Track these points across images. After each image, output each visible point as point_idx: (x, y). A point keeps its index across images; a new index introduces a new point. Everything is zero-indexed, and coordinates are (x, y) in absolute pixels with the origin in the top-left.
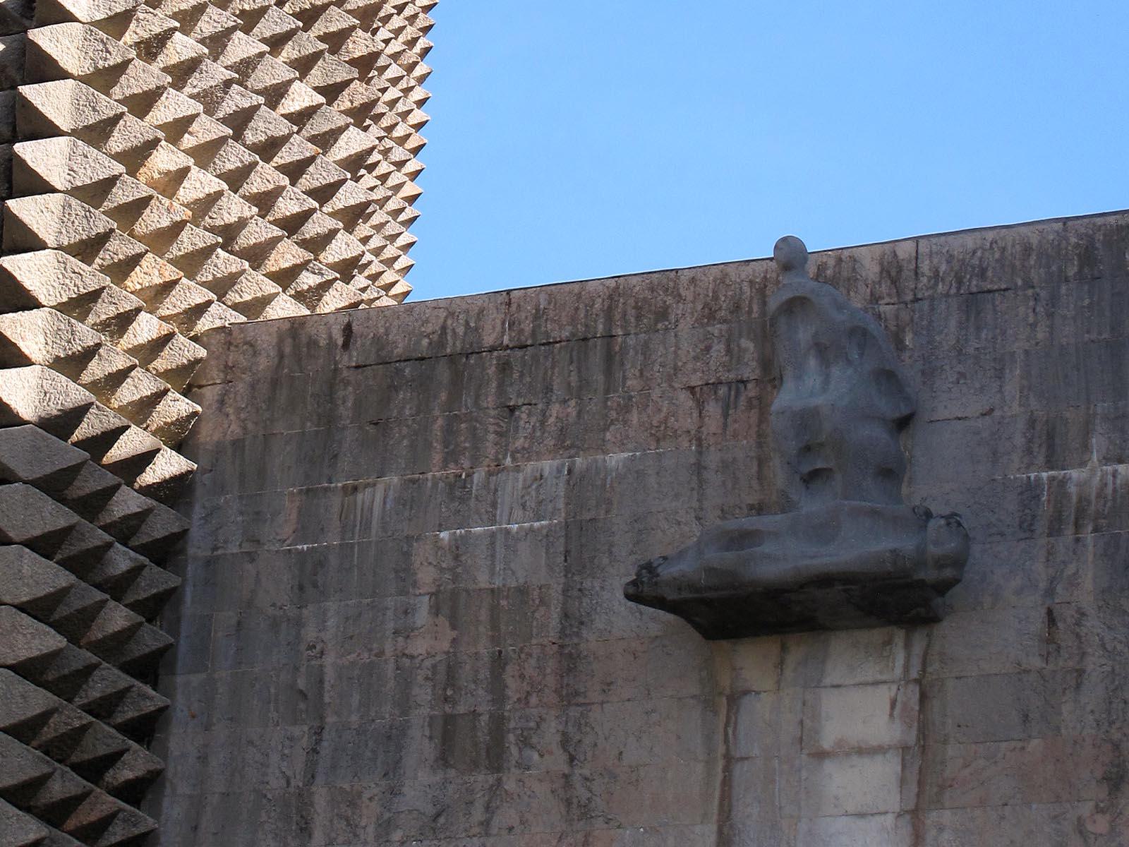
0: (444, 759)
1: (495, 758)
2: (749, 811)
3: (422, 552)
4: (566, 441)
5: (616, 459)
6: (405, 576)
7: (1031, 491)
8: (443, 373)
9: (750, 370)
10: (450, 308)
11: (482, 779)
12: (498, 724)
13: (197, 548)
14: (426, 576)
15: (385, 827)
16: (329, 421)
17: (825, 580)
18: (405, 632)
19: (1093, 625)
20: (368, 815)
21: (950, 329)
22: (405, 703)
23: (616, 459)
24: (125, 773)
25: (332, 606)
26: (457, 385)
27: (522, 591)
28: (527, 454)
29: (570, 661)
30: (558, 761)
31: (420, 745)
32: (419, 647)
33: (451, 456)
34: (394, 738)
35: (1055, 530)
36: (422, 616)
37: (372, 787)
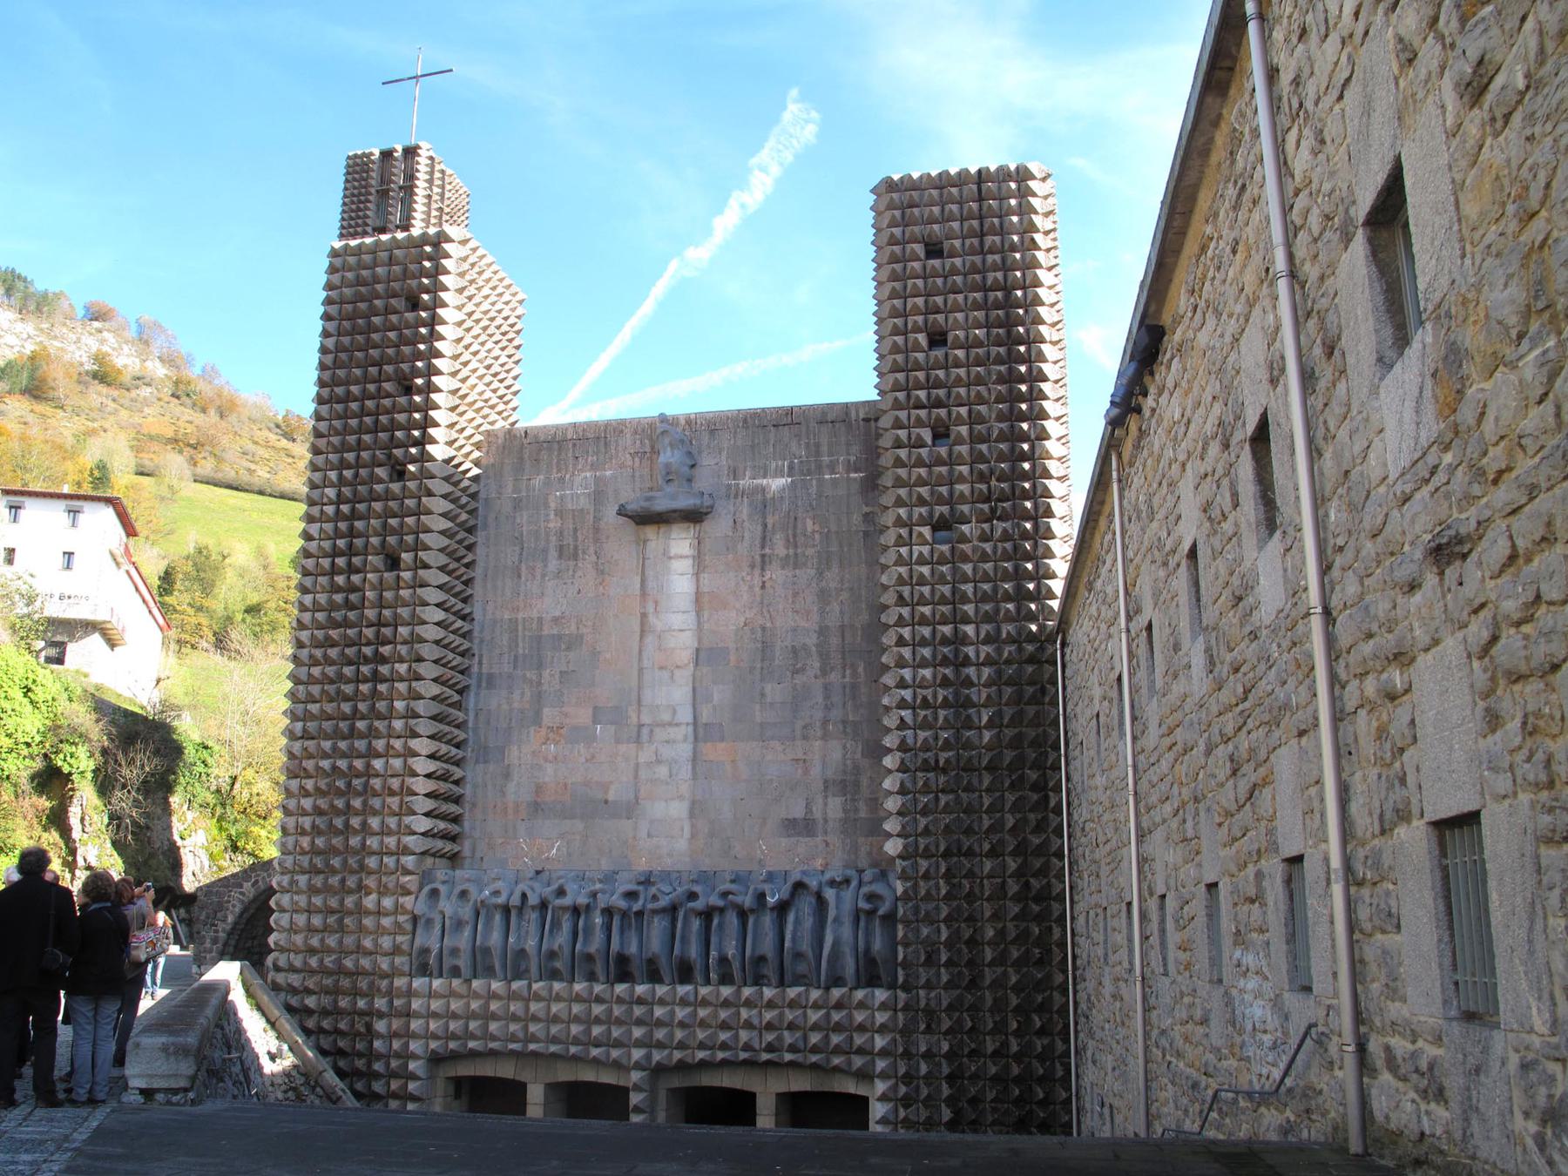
0: (560, 556)
1: (575, 557)
2: (650, 573)
3: (551, 498)
4: (593, 467)
5: (608, 473)
6: (546, 505)
7: (729, 486)
8: (556, 446)
9: (648, 449)
10: (557, 427)
11: (572, 563)
12: (576, 548)
13: (482, 495)
14: (553, 505)
15: (543, 576)
16: (521, 459)
17: (675, 511)
18: (547, 521)
19: (746, 524)
20: (538, 572)
21: (706, 438)
22: (548, 541)
23: (608, 473)
24: (466, 561)
25: (525, 513)
26: (560, 449)
28: (582, 471)
29: (597, 530)
30: (594, 558)
31: (553, 553)
32: (551, 525)
33: (559, 471)
34: (545, 551)
35: (736, 497)
36: (552, 516)
37: (539, 565)
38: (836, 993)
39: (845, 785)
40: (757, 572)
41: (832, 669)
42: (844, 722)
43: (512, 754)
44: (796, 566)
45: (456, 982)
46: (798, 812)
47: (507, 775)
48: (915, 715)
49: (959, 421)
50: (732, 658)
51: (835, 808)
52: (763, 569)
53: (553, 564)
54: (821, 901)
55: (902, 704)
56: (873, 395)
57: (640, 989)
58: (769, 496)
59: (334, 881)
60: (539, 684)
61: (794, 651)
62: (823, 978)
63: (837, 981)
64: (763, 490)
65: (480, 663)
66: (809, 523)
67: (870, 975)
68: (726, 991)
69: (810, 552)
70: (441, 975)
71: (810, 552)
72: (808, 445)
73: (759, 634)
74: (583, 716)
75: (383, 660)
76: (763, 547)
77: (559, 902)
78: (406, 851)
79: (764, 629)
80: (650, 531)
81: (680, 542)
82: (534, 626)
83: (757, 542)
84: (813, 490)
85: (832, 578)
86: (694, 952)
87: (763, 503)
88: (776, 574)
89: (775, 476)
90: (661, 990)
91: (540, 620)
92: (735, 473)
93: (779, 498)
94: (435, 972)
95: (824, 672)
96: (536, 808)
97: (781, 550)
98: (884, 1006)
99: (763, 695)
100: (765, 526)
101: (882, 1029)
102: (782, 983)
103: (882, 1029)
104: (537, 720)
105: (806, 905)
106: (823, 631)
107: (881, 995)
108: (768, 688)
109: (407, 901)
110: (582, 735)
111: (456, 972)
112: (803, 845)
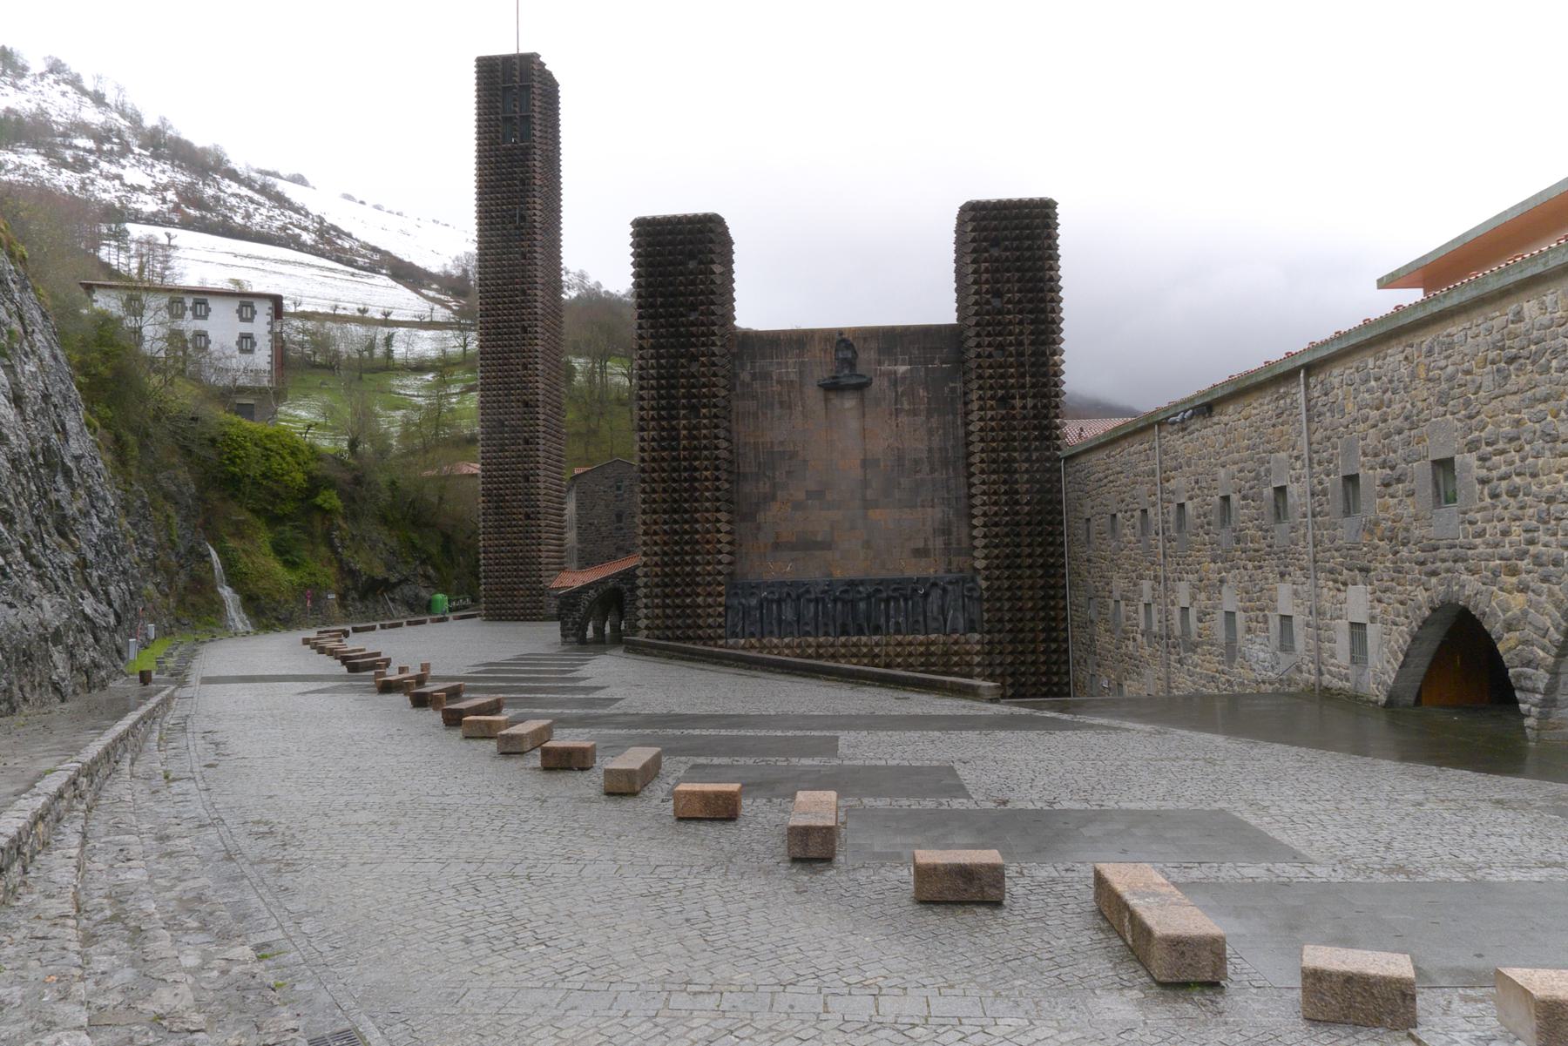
1: (790, 407)
6: (772, 379)
11: (788, 411)
12: (790, 402)
14: (775, 378)
15: (772, 418)
20: (769, 416)
27: (792, 381)
30: (801, 408)
31: (777, 405)
32: (774, 389)
36: (775, 384)
38: (955, 636)
39: (945, 530)
40: (894, 417)
41: (935, 470)
42: (943, 499)
43: (761, 517)
44: (915, 415)
45: (753, 640)
46: (921, 545)
47: (759, 528)
48: (990, 498)
49: (1011, 344)
50: (882, 464)
51: (939, 542)
52: (897, 416)
53: (777, 411)
54: (944, 590)
55: (984, 493)
56: (955, 322)
57: (855, 639)
58: (899, 376)
59: (678, 590)
60: (774, 478)
61: (916, 462)
62: (948, 629)
63: (955, 631)
64: (895, 372)
65: (738, 467)
66: (921, 391)
67: (971, 627)
68: (899, 638)
69: (922, 407)
70: (743, 637)
71: (922, 407)
72: (918, 348)
73: (896, 451)
74: (801, 496)
75: (696, 469)
76: (896, 404)
77: (808, 596)
78: (720, 573)
79: (898, 449)
80: (832, 395)
81: (849, 402)
82: (769, 445)
83: (893, 401)
84: (922, 374)
85: (934, 422)
86: (883, 620)
87: (895, 381)
88: (903, 419)
89: (902, 365)
90: (864, 639)
91: (772, 442)
92: (880, 363)
93: (904, 378)
94: (740, 634)
95: (932, 470)
96: (777, 546)
97: (906, 406)
98: (978, 642)
99: (899, 484)
100: (897, 392)
101: (977, 653)
102: (926, 633)
103: (977, 653)
104: (774, 498)
105: (935, 594)
106: (930, 450)
107: (977, 637)
108: (902, 480)
109: (722, 599)
110: (798, 506)
111: (752, 635)
112: (923, 562)
